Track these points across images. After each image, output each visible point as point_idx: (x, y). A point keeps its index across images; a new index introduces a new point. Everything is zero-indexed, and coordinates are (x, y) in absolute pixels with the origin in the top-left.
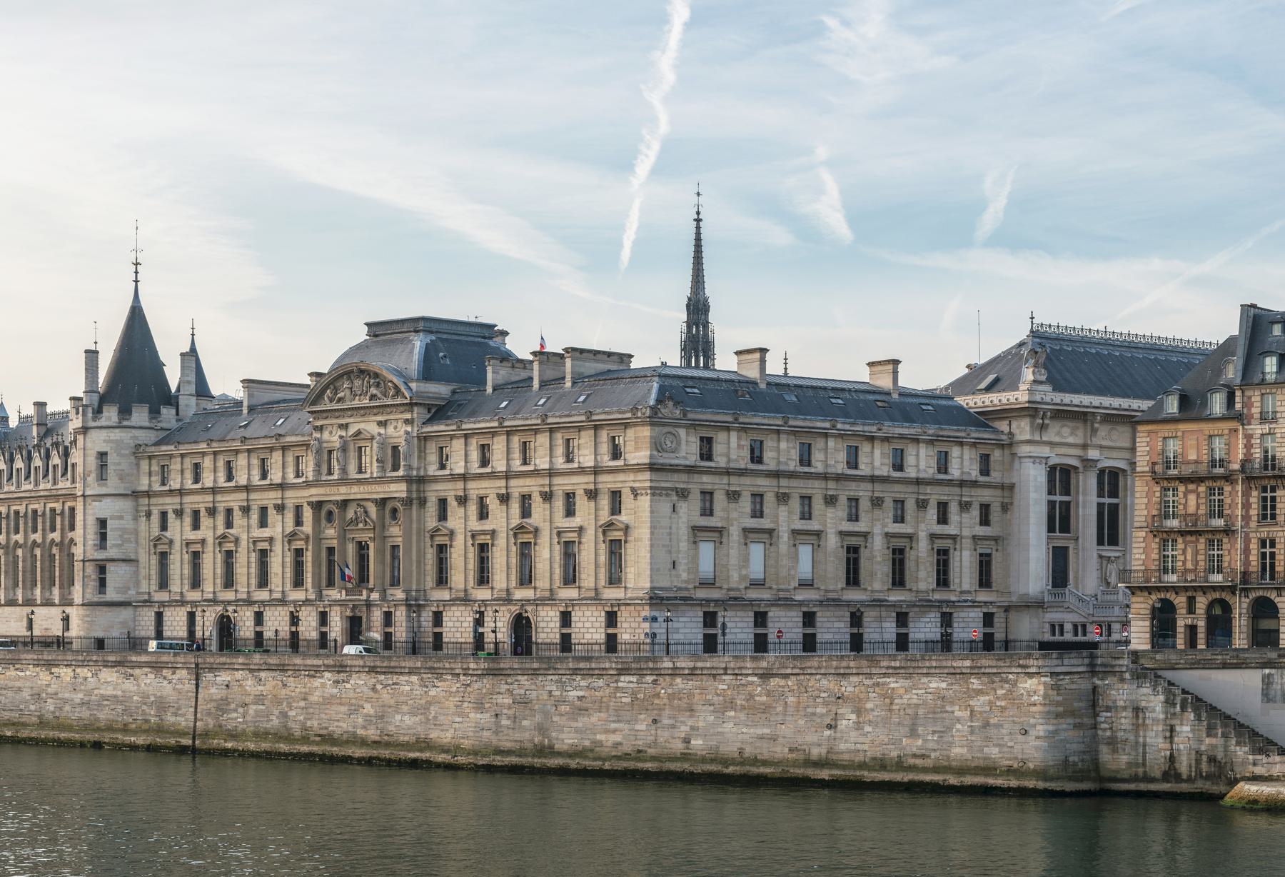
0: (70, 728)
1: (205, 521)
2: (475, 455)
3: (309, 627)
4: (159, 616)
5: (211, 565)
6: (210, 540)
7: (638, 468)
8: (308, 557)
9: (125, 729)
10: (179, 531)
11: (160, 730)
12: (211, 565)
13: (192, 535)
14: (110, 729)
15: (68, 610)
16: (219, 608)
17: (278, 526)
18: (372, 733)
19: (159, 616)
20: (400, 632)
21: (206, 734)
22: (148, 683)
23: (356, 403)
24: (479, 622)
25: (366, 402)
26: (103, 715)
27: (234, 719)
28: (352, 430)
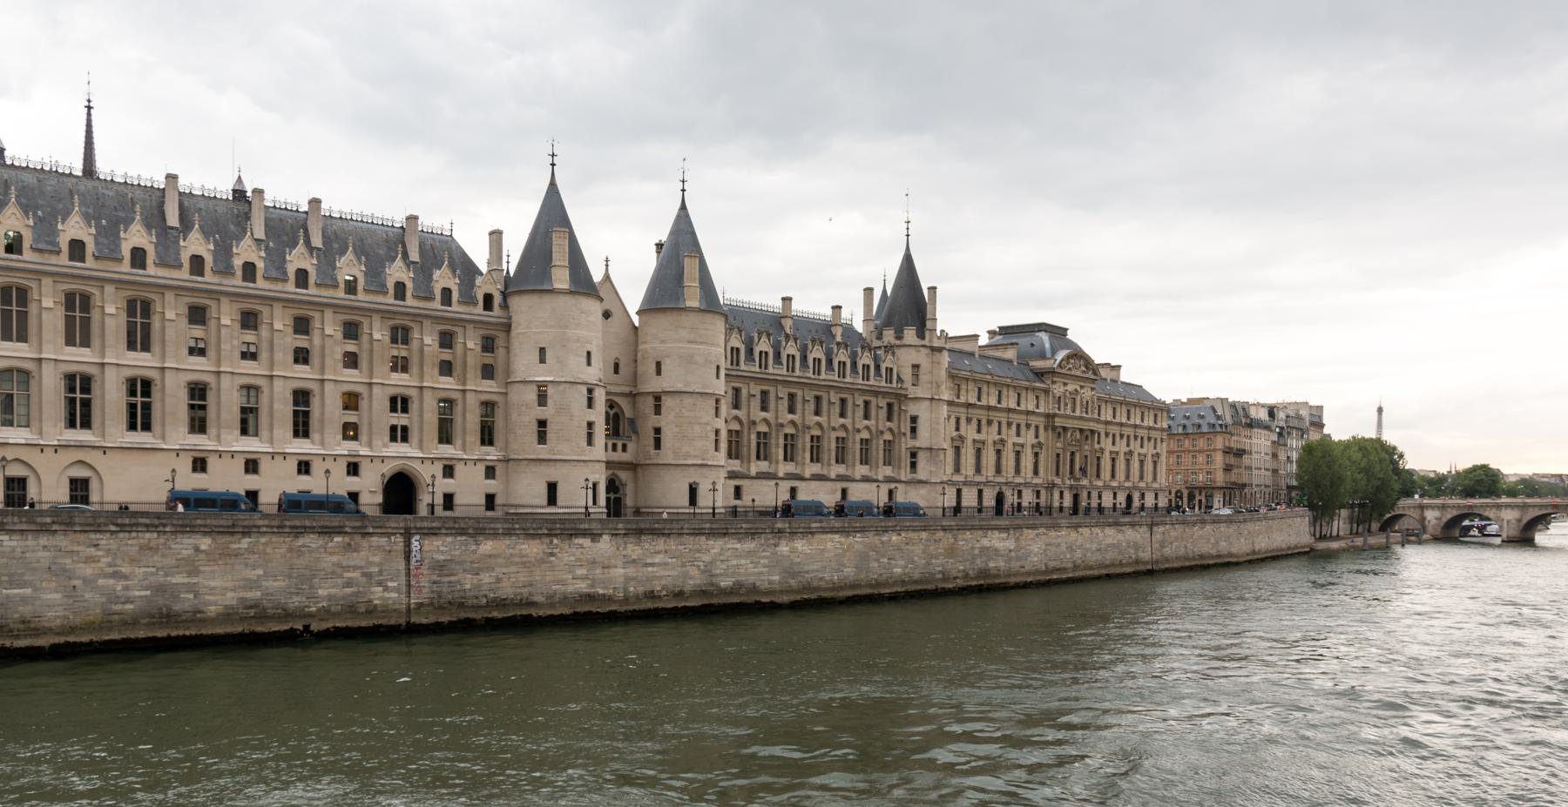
0: (1091, 568)
1: (984, 428)
2: (1110, 412)
3: (1043, 501)
4: (959, 491)
5: (989, 457)
6: (990, 441)
7: (1162, 430)
8: (1042, 457)
9: (1121, 564)
10: (970, 432)
11: (1137, 562)
12: (989, 457)
13: (977, 437)
14: (1113, 565)
15: (893, 486)
16: (997, 489)
17: (1028, 438)
18: (1214, 552)
19: (959, 491)
20: (1094, 504)
21: (1157, 562)
22: (1131, 535)
23: (1073, 372)
24: (1038, 497)
25: (1078, 373)
26: (1110, 556)
27: (1168, 551)
28: (1070, 388)
